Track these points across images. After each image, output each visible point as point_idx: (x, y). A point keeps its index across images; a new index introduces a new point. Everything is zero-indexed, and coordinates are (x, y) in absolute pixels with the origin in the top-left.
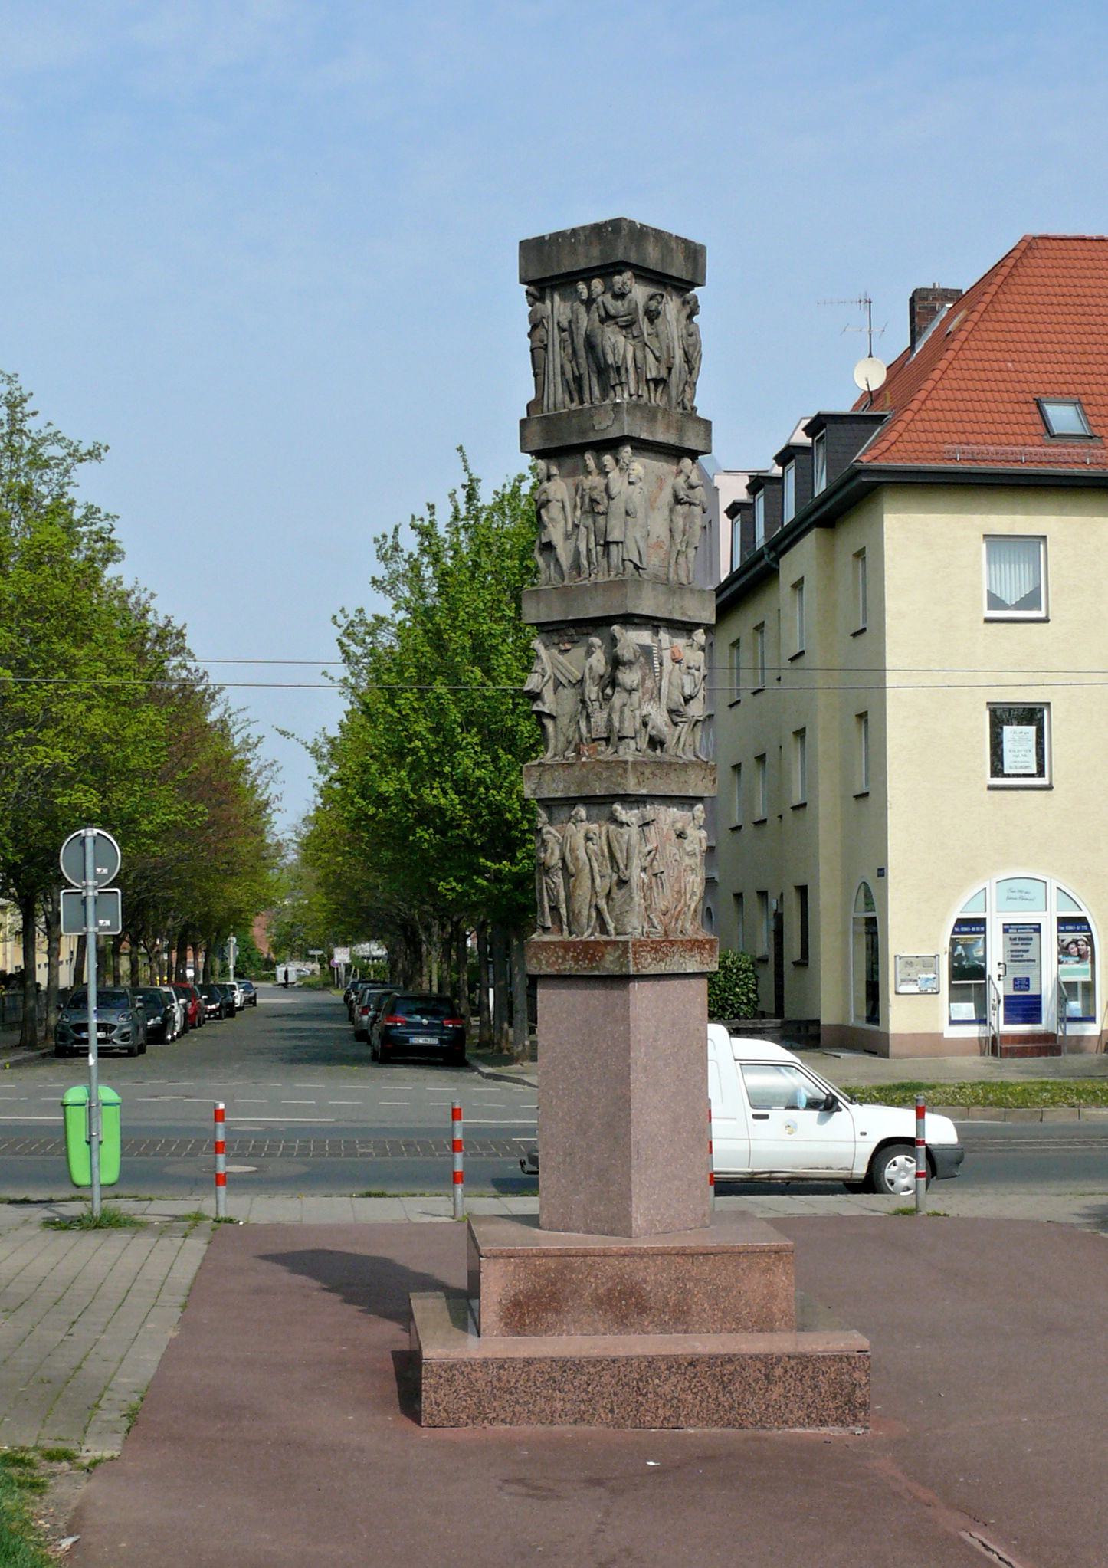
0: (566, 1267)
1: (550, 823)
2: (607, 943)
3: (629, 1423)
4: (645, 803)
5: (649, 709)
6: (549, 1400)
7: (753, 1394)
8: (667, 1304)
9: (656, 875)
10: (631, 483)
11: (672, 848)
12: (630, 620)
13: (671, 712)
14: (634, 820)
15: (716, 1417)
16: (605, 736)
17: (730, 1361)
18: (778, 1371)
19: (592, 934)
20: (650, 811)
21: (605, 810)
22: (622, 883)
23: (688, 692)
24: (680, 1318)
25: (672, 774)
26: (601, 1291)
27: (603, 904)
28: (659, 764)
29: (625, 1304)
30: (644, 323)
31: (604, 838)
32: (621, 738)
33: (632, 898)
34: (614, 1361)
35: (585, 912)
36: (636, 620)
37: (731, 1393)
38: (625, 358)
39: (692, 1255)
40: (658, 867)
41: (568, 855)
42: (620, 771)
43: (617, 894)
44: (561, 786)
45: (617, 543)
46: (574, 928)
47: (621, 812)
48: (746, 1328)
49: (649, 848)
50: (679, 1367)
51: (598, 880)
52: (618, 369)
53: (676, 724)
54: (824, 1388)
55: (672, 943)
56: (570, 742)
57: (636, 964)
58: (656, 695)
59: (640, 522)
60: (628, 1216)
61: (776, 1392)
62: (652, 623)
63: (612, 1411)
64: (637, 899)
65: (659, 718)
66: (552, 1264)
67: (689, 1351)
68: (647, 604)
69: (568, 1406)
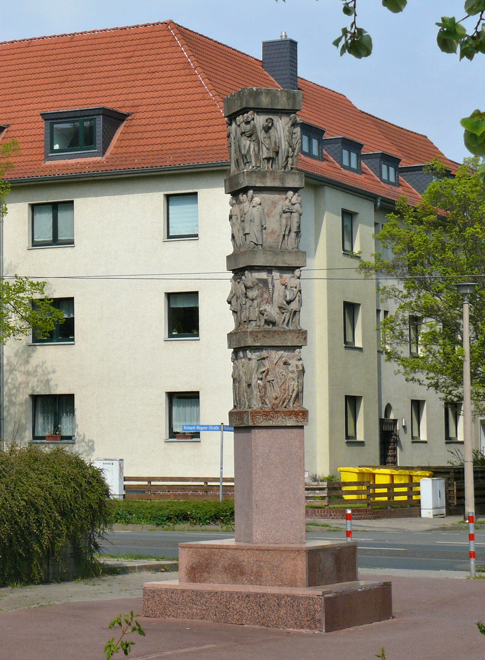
0: (211, 553)
3: (222, 621)
4: (262, 349)
5: (267, 307)
6: (191, 608)
7: (273, 611)
8: (253, 572)
9: (269, 381)
10: (254, 207)
11: (280, 369)
12: (252, 268)
13: (280, 308)
14: (254, 357)
15: (257, 621)
17: (263, 596)
18: (283, 602)
20: (264, 353)
23: (288, 298)
24: (258, 579)
25: (277, 336)
26: (226, 565)
28: (268, 332)
29: (236, 571)
30: (262, 135)
32: (250, 321)
34: (216, 593)
36: (256, 268)
37: (263, 610)
38: (249, 150)
39: (263, 550)
40: (269, 378)
43: (249, 390)
45: (248, 234)
47: (249, 354)
48: (285, 585)
49: (263, 370)
50: (242, 598)
52: (245, 156)
53: (283, 313)
54: (302, 611)
55: (277, 412)
57: (253, 421)
58: (270, 301)
59: (256, 224)
60: (251, 535)
61: (283, 611)
62: (269, 269)
63: (216, 615)
64: (255, 392)
65: (272, 311)
66: (206, 551)
67: (247, 590)
68: (260, 261)
69: (199, 611)
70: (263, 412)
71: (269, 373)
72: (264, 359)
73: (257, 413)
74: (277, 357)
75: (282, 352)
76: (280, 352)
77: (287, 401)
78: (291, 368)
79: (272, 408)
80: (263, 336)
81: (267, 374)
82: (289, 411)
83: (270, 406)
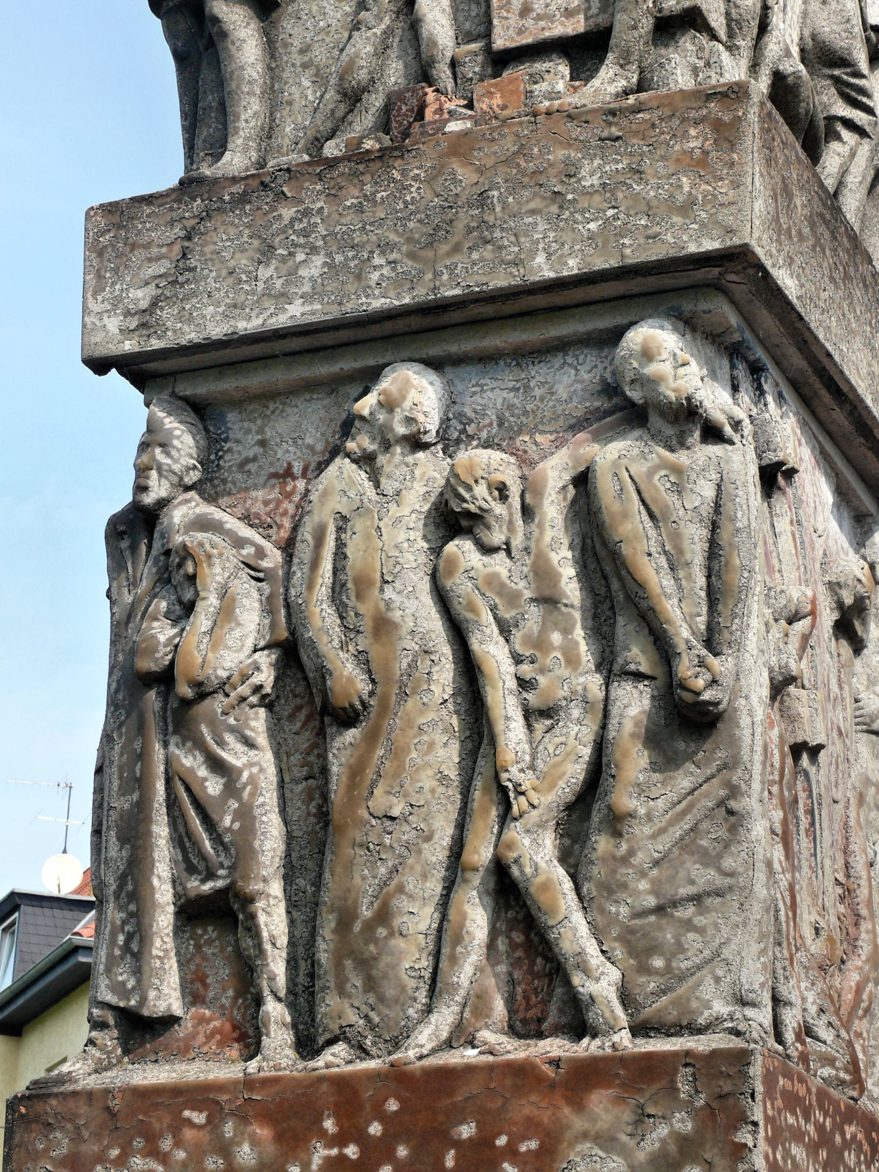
1: (209, 483)
2: (583, 1077)
16: (576, 26)
19: (461, 1035)
21: (569, 382)
22: (689, 722)
27: (538, 854)
31: (553, 510)
33: (733, 818)
35: (418, 917)
41: (322, 619)
42: (695, 140)
44: (315, 267)
46: (338, 1008)
51: (512, 733)
56: (353, 98)
64: (759, 829)
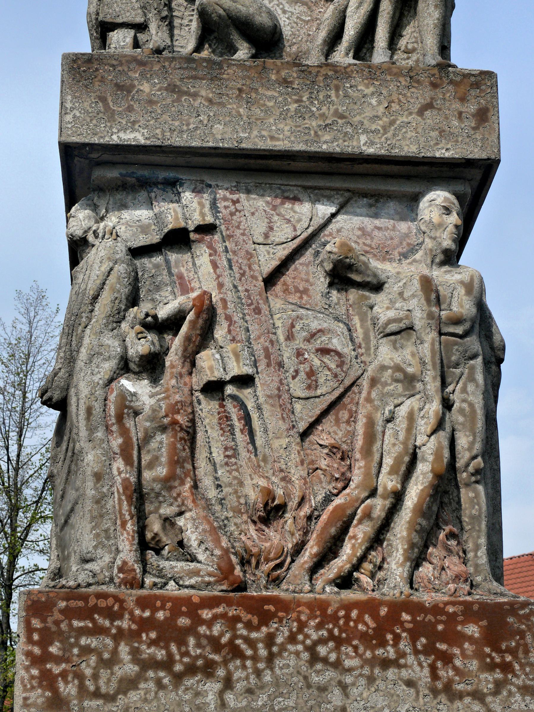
9: (213, 388)
20: (189, 207)
55: (263, 612)
70: (143, 603)
71: (220, 333)
72: (178, 239)
73: (87, 613)
74: (283, 232)
75: (325, 209)
76: (304, 209)
77: (360, 532)
78: (385, 308)
79: (226, 572)
80: (172, 89)
81: (204, 336)
82: (370, 607)
83: (206, 562)
